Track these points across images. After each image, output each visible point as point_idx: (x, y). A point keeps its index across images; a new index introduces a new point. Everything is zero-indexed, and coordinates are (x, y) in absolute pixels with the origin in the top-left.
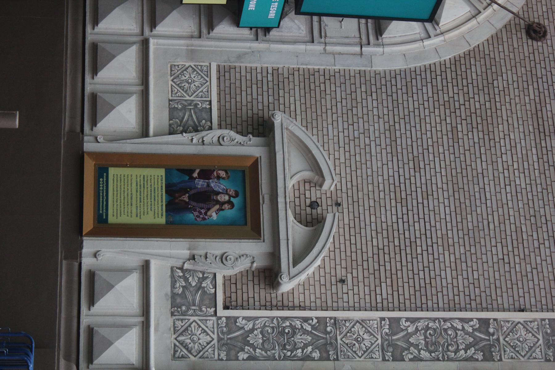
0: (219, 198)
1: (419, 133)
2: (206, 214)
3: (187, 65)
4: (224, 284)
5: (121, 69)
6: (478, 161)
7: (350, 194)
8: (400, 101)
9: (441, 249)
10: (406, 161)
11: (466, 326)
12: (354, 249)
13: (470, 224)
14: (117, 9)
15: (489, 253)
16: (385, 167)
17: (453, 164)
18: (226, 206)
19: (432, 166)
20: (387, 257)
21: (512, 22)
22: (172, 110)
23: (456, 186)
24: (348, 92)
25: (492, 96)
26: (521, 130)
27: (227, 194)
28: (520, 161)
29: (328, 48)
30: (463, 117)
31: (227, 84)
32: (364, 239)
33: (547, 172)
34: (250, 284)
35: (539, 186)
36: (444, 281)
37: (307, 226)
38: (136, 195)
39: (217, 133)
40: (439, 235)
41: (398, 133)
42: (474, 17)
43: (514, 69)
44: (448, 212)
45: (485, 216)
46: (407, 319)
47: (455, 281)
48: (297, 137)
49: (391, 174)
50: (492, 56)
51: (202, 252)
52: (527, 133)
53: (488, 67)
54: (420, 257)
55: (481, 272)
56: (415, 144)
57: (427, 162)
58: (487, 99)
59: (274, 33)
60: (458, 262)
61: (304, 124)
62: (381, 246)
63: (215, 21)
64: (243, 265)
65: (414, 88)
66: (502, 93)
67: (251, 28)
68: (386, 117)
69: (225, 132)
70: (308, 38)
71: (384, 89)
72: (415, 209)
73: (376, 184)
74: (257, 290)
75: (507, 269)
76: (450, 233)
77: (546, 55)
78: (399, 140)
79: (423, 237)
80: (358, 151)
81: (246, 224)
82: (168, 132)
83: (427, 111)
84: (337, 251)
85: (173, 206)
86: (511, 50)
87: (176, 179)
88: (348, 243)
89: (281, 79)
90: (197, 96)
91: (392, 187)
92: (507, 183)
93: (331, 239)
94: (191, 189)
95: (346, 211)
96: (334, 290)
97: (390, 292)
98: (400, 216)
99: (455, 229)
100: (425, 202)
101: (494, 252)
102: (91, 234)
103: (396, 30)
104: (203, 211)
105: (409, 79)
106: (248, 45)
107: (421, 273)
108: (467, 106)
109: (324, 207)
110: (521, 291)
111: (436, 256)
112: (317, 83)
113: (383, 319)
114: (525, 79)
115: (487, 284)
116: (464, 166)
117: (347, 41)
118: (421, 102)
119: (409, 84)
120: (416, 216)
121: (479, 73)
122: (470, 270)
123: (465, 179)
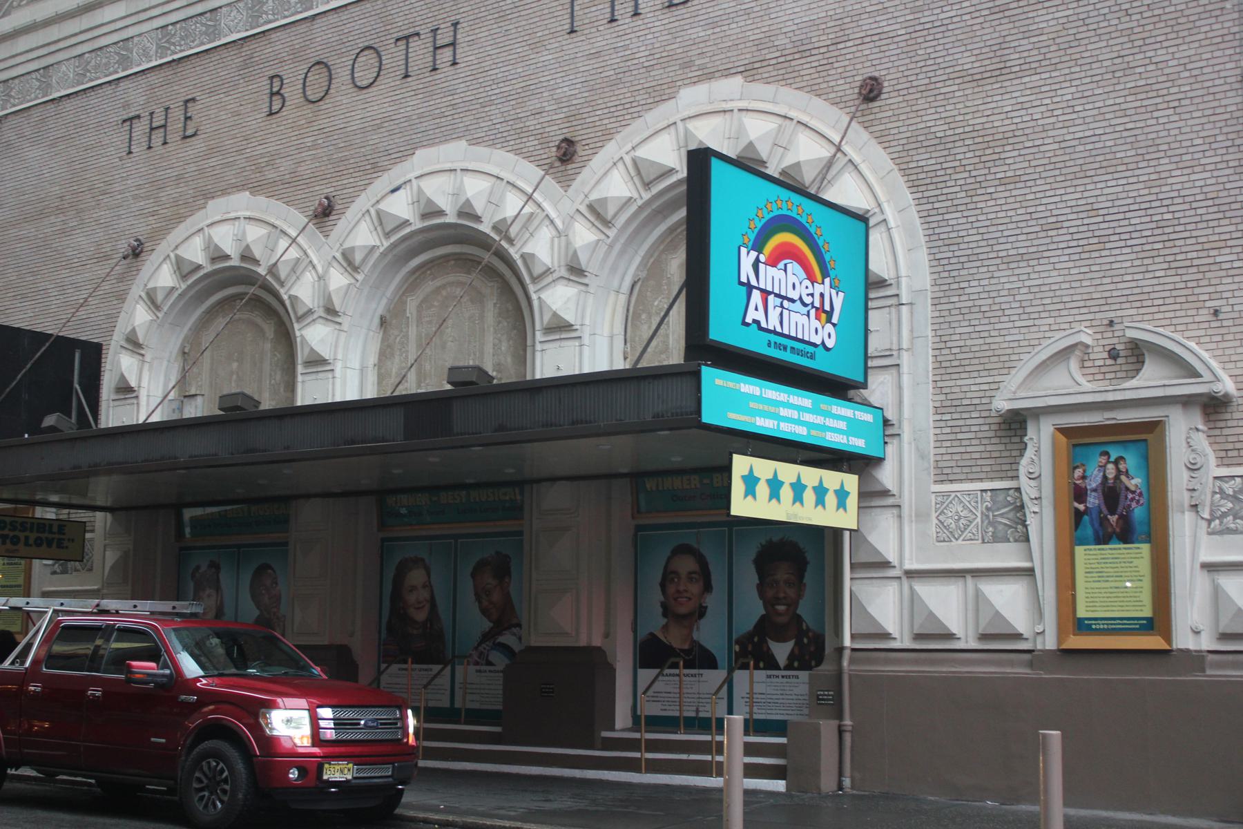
0: (1110, 476)
1: (1010, 226)
2: (1133, 492)
3: (935, 521)
4: (1228, 465)
5: (948, 606)
6: (1042, 148)
7: (1097, 309)
8: (969, 252)
9: (1164, 189)
10: (1048, 240)
12: (1171, 300)
13: (1129, 153)
14: (869, 610)
15: (1167, 126)
16: (1057, 266)
17: (1049, 180)
18: (1122, 467)
19: (1053, 206)
20: (1179, 257)
21: (860, 120)
22: (996, 539)
23: (1078, 175)
24: (960, 317)
25: (957, 138)
26: (999, 98)
27: (1104, 466)
28: (1040, 96)
29: (905, 345)
30: (986, 171)
31: (958, 470)
32: (1157, 288)
33: (1053, 61)
35: (1073, 70)
36: (1209, 182)
37: (1143, 362)
38: (1112, 582)
39: (1024, 482)
40: (1146, 192)
41: (1011, 252)
42: (856, 167)
43: (920, 113)
44: (1114, 183)
45: (1117, 135)
47: (1208, 168)
48: (1025, 380)
49: (1066, 258)
50: (904, 141)
51: (1186, 495)
52: (1003, 91)
53: (919, 145)
54: (1177, 215)
55: (1194, 135)
56: (1025, 231)
57: (1048, 214)
58: (961, 143)
59: (890, 415)
60: (1181, 165)
61: (1006, 371)
62: (1165, 266)
63: (878, 488)
64: (1201, 441)
65: (952, 235)
66: (952, 126)
67: (886, 443)
68: (991, 268)
69: (1022, 471)
70: (894, 371)
71: (953, 274)
72: (1112, 225)
73: (1081, 277)
74: (1235, 423)
75: (1187, 102)
76: (1141, 179)
77: (900, 75)
78: (1021, 251)
79: (1150, 212)
80: (1038, 302)
81: (1145, 440)
82: (1022, 545)
83: (980, 218)
84: (1175, 321)
85: (1126, 534)
86: (895, 118)
87: (1088, 529)
88: (1163, 308)
89: (949, 403)
90: (976, 508)
91: (1083, 256)
92: (1070, 110)
93: (1160, 330)
94: (1101, 512)
95: (1119, 313)
96: (1230, 323)
97: (1227, 251)
98: (1122, 244)
99: (1137, 172)
100: (1101, 212)
101: (1165, 120)
102: (1168, 637)
103: (879, 265)
104: (1130, 496)
105: (940, 243)
106: (906, 446)
107: (1199, 211)
108: (971, 167)
109: (1115, 341)
110: (1217, 82)
111: (1175, 194)
112: (952, 357)
114: (932, 99)
115: (1211, 126)
116: (1052, 167)
117: (895, 323)
118: (969, 226)
119: (947, 242)
120: (1122, 223)
121: (928, 156)
122: (1191, 150)
123: (1068, 164)
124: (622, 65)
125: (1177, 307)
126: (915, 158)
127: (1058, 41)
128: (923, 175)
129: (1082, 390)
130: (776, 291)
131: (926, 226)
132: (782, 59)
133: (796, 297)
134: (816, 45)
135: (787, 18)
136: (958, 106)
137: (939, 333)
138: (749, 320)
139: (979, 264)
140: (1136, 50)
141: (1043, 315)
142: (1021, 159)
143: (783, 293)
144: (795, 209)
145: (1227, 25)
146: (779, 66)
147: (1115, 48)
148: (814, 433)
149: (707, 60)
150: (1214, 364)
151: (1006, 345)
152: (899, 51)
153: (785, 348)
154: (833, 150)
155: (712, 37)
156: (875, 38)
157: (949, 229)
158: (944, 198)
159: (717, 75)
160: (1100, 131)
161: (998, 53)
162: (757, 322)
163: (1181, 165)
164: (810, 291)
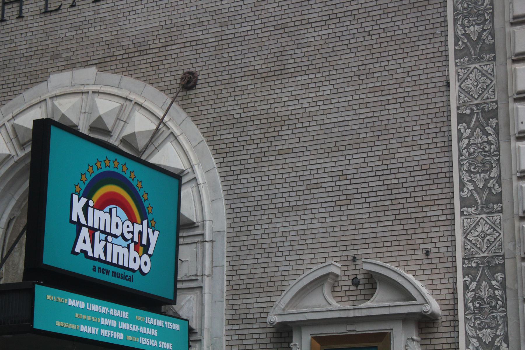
1: (284, 185)
6: (309, 129)
7: (344, 248)
8: (255, 203)
9: (393, 161)
10: (311, 197)
11: (465, 135)
12: (397, 243)
13: (369, 135)
15: (396, 116)
17: (312, 152)
19: (315, 172)
21: (181, 103)
23: (333, 149)
24: (247, 252)
25: (249, 119)
28: (308, 91)
29: (207, 272)
30: (269, 144)
32: (386, 234)
33: (318, 66)
34: (434, 341)
35: (331, 73)
36: (423, 157)
37: (376, 289)
40: (380, 163)
41: (285, 205)
42: (176, 138)
43: (223, 100)
44: (358, 156)
45: (361, 121)
46: (461, 190)
47: (423, 147)
49: (323, 210)
50: (212, 120)
53: (222, 123)
55: (414, 123)
57: (312, 177)
58: (251, 123)
59: (194, 325)
60: (404, 144)
62: (393, 218)
66: (246, 110)
67: (190, 346)
68: (270, 216)
70: (198, 292)
71: (244, 219)
73: (334, 224)
74: (439, 335)
75: (409, 99)
76: (377, 153)
77: (210, 71)
79: (383, 178)
80: (303, 242)
81: (376, 347)
83: (264, 178)
84: (398, 259)
86: (206, 103)
88: (390, 249)
89: (237, 317)
91: (336, 209)
92: (329, 102)
93: (388, 265)
95: (360, 252)
96: (437, 261)
97: (436, 208)
98: (363, 200)
99: (374, 149)
100: (349, 177)
103: (189, 209)
105: (235, 196)
107: (417, 178)
108: (259, 141)
109: (357, 272)
110: (430, 86)
111: (400, 165)
112: (240, 282)
113: (462, 214)
114: (232, 90)
115: (425, 117)
116: (315, 142)
117: (200, 255)
118: (256, 184)
119: (239, 196)
120: (363, 185)
121: (228, 131)
122: (411, 134)
123: (326, 141)
124: (8, 54)
125: (401, 248)
126: (218, 133)
127: (321, 51)
128: (224, 146)
129: (331, 308)
130: (102, 228)
131: (225, 183)
132: (125, 56)
133: (118, 233)
134: (151, 47)
135: (130, 26)
136: (250, 96)
137: (232, 263)
138: (77, 250)
139: (261, 212)
140: (375, 60)
141: (306, 252)
142: (294, 136)
143: (108, 230)
144: (120, 167)
145: (436, 45)
146: (124, 61)
147: (360, 59)
148: (129, 337)
149: (71, 54)
150: (425, 291)
151: (279, 274)
152: (210, 54)
153: (108, 272)
154: (157, 123)
155: (76, 37)
156: (194, 43)
157: (242, 186)
158: (238, 163)
159: (78, 65)
160: (349, 118)
161: (280, 58)
162: (84, 252)
163: (404, 144)
164: (131, 229)
